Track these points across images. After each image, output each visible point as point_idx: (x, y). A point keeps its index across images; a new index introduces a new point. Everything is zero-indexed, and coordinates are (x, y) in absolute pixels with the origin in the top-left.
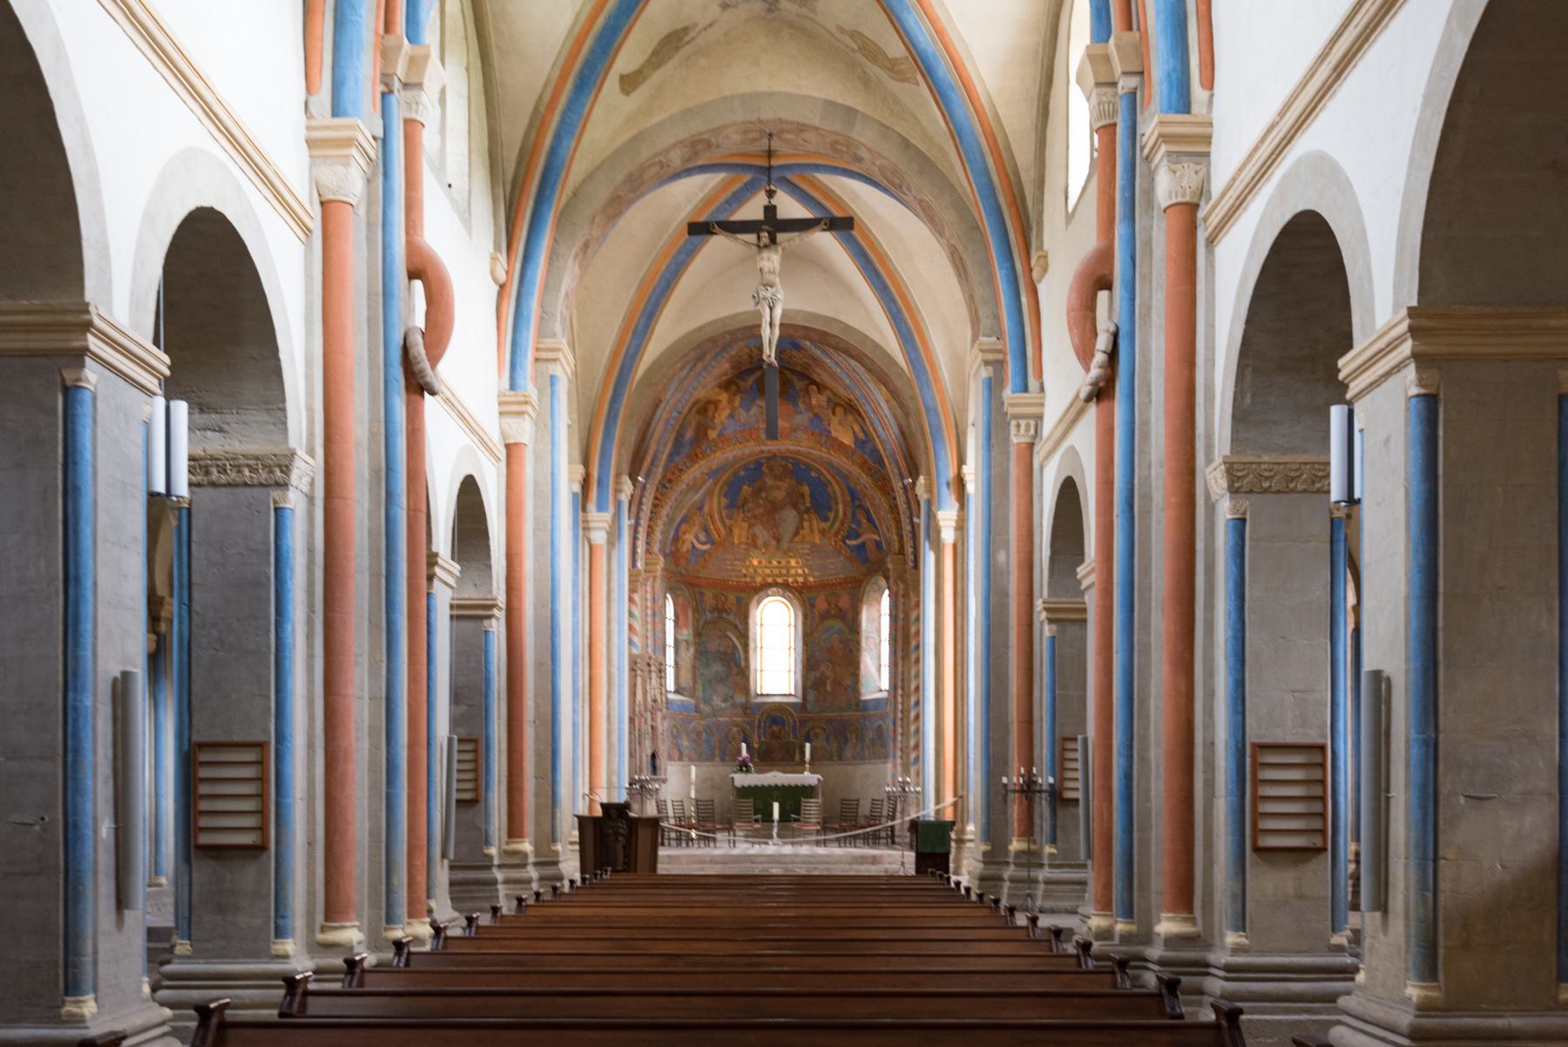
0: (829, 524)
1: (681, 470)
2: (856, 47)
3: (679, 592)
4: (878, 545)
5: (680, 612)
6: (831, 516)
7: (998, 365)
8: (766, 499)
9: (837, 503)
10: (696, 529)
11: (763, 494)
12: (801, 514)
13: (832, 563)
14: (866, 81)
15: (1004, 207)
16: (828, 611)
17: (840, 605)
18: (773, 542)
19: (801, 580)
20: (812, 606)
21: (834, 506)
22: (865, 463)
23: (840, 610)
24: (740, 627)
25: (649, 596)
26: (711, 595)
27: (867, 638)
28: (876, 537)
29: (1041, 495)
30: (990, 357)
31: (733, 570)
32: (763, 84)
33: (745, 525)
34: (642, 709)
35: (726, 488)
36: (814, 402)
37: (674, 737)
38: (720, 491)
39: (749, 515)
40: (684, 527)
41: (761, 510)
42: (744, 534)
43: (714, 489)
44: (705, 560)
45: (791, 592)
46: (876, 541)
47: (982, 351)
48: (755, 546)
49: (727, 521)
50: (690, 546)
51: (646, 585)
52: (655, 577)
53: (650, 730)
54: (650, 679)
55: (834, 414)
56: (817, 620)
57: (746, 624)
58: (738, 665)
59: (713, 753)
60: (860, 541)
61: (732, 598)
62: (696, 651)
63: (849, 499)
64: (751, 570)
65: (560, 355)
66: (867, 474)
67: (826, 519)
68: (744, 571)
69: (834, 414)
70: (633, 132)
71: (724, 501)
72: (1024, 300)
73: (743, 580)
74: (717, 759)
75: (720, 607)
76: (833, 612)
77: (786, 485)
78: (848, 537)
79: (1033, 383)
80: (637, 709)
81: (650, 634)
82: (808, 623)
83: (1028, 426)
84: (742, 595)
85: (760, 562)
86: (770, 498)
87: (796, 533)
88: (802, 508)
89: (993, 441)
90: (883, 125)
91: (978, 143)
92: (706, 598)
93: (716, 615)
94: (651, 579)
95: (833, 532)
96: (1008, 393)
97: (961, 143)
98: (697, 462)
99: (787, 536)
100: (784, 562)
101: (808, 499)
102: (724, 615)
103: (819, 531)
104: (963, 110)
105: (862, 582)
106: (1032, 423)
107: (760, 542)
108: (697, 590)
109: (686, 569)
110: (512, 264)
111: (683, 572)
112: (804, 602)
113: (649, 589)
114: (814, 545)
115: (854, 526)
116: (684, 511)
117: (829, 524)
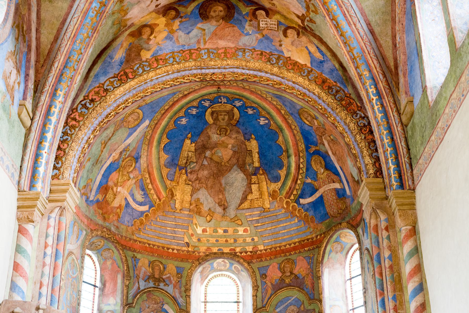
0: (280, 184)
1: (106, 90)
3: (106, 254)
4: (340, 194)
6: (283, 173)
8: (211, 159)
9: (289, 157)
10: (131, 182)
11: (208, 153)
12: (249, 176)
13: (284, 228)
16: (282, 280)
17: (296, 272)
18: (219, 210)
19: (250, 249)
20: (264, 276)
21: (285, 162)
22: (324, 82)
23: (296, 277)
27: (331, 307)
28: (337, 186)
31: (174, 238)
33: (189, 189)
35: (165, 140)
36: (262, 25)
38: (159, 143)
39: (193, 177)
40: (114, 176)
41: (206, 173)
42: (188, 198)
43: (152, 137)
44: (142, 223)
45: (238, 262)
46: (337, 190)
48: (199, 213)
49: (168, 182)
50: (123, 203)
55: (286, 36)
56: (270, 292)
60: (317, 195)
61: (171, 266)
63: (302, 146)
64: (194, 239)
66: (328, 94)
67: (276, 179)
68: (186, 240)
69: (286, 36)
71: (165, 157)
73: (185, 248)
76: (287, 281)
77: (232, 141)
78: (302, 196)
81: (45, 281)
82: (259, 294)
84: (186, 265)
85: (204, 231)
86: (215, 158)
87: (244, 199)
88: (250, 169)
95: (284, 193)
98: (126, 82)
99: (234, 202)
100: (231, 230)
101: (256, 156)
102: (162, 285)
103: (270, 195)
105: (321, 242)
107: (205, 208)
111: (113, 229)
112: (254, 272)
113: (52, 222)
114: (264, 210)
115: (309, 181)
116: (115, 155)
117: (280, 184)
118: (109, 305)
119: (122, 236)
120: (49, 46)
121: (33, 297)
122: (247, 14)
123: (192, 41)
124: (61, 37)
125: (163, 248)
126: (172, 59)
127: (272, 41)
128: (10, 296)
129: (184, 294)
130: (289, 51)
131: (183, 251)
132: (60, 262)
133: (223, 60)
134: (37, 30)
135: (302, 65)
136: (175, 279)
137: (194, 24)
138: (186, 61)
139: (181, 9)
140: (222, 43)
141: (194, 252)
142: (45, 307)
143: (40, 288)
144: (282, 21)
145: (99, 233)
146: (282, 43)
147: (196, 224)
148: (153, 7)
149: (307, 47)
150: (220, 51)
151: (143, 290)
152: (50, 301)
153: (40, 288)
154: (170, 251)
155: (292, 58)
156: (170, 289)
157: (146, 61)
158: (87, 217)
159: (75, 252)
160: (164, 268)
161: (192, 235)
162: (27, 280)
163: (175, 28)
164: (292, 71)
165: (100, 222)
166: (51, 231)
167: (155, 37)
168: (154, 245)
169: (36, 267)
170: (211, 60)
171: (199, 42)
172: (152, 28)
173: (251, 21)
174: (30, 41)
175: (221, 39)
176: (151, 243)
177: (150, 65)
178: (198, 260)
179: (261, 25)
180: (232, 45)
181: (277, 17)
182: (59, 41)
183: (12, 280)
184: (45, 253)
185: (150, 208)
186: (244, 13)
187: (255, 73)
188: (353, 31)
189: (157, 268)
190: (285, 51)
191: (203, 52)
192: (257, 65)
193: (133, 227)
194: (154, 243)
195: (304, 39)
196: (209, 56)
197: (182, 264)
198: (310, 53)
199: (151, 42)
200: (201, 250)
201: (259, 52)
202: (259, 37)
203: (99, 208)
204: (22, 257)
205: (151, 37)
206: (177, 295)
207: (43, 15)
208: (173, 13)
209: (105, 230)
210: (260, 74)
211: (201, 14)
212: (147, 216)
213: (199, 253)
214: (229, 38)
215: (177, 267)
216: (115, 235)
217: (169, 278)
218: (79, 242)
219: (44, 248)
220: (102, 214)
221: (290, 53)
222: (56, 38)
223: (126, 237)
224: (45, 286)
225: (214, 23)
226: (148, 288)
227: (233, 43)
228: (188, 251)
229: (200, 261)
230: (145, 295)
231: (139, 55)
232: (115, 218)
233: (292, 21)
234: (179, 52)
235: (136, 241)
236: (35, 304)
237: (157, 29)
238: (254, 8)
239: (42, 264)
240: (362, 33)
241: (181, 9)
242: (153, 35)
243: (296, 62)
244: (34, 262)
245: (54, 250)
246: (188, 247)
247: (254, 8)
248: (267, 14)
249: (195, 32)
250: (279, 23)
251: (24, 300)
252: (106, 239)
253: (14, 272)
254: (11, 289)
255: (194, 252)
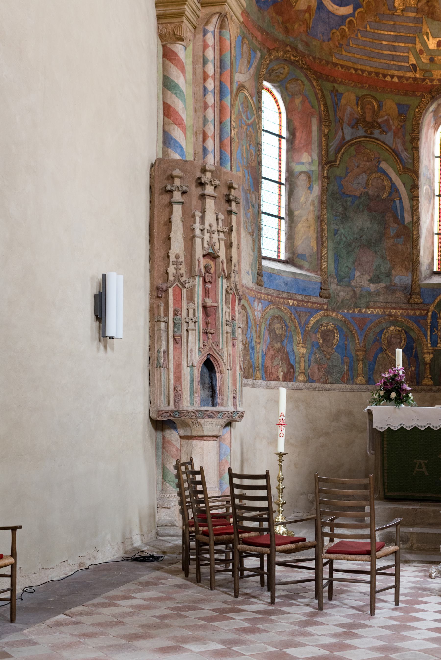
5: (297, 123)
24: (405, 155)
25: (210, 54)
26: (353, 98)
34: (183, 270)
37: (275, 337)
44: (343, 35)
51: (205, 33)
52: (223, 17)
53: (200, 313)
54: (203, 212)
57: (417, 149)
58: (399, 221)
59: (351, 368)
62: (324, 190)
64: (425, 59)
68: (412, 61)
74: (360, 379)
75: (369, 119)
80: (172, 270)
81: (211, 129)
92: (343, 101)
93: (361, 132)
94: (215, 19)
108: (328, 85)
109: (307, 44)
111: (300, 47)
118: (303, 163)
119: (314, 58)
121: (195, 155)
125: (377, 74)
128: (165, 153)
129: (409, 146)
131: (408, 79)
132: (227, 101)
136: (396, 123)
141: (424, 80)
142: (213, 168)
143: (204, 141)
145: (281, 54)
147: (427, 34)
151: (349, 141)
152: (219, 159)
153: (204, 141)
154: (388, 79)
156: (389, 138)
158: (260, 28)
159: (247, 85)
160: (380, 107)
161: (421, 52)
162: (184, 130)
165: (281, 36)
166: (210, 54)
168: (363, 71)
169: (195, 110)
176: (359, 67)
178: (430, 92)
183: (164, 131)
184: (205, 89)
185: (355, 9)
189: (369, 106)
193: (331, 43)
194: (363, 68)
197: (406, 100)
200: (435, 76)
203: (277, 13)
204: (174, 96)
206: (400, 147)
209: (288, 48)
212: (351, 22)
213: (432, 80)
215: (398, 105)
216: (303, 56)
217: (387, 121)
218: (252, 70)
219: (202, 82)
220: (283, 23)
223: (321, 60)
224: (210, 138)
226: (356, 138)
228: (415, 79)
229: (434, 94)
230: (353, 148)
232: (303, 29)
235: (336, 65)
236: (199, 163)
239: (202, 104)
244: (190, 101)
245: (217, 83)
246: (416, 71)
251: (184, 159)
252: (292, 63)
253: (166, 119)
254: (164, 143)
255: (424, 80)
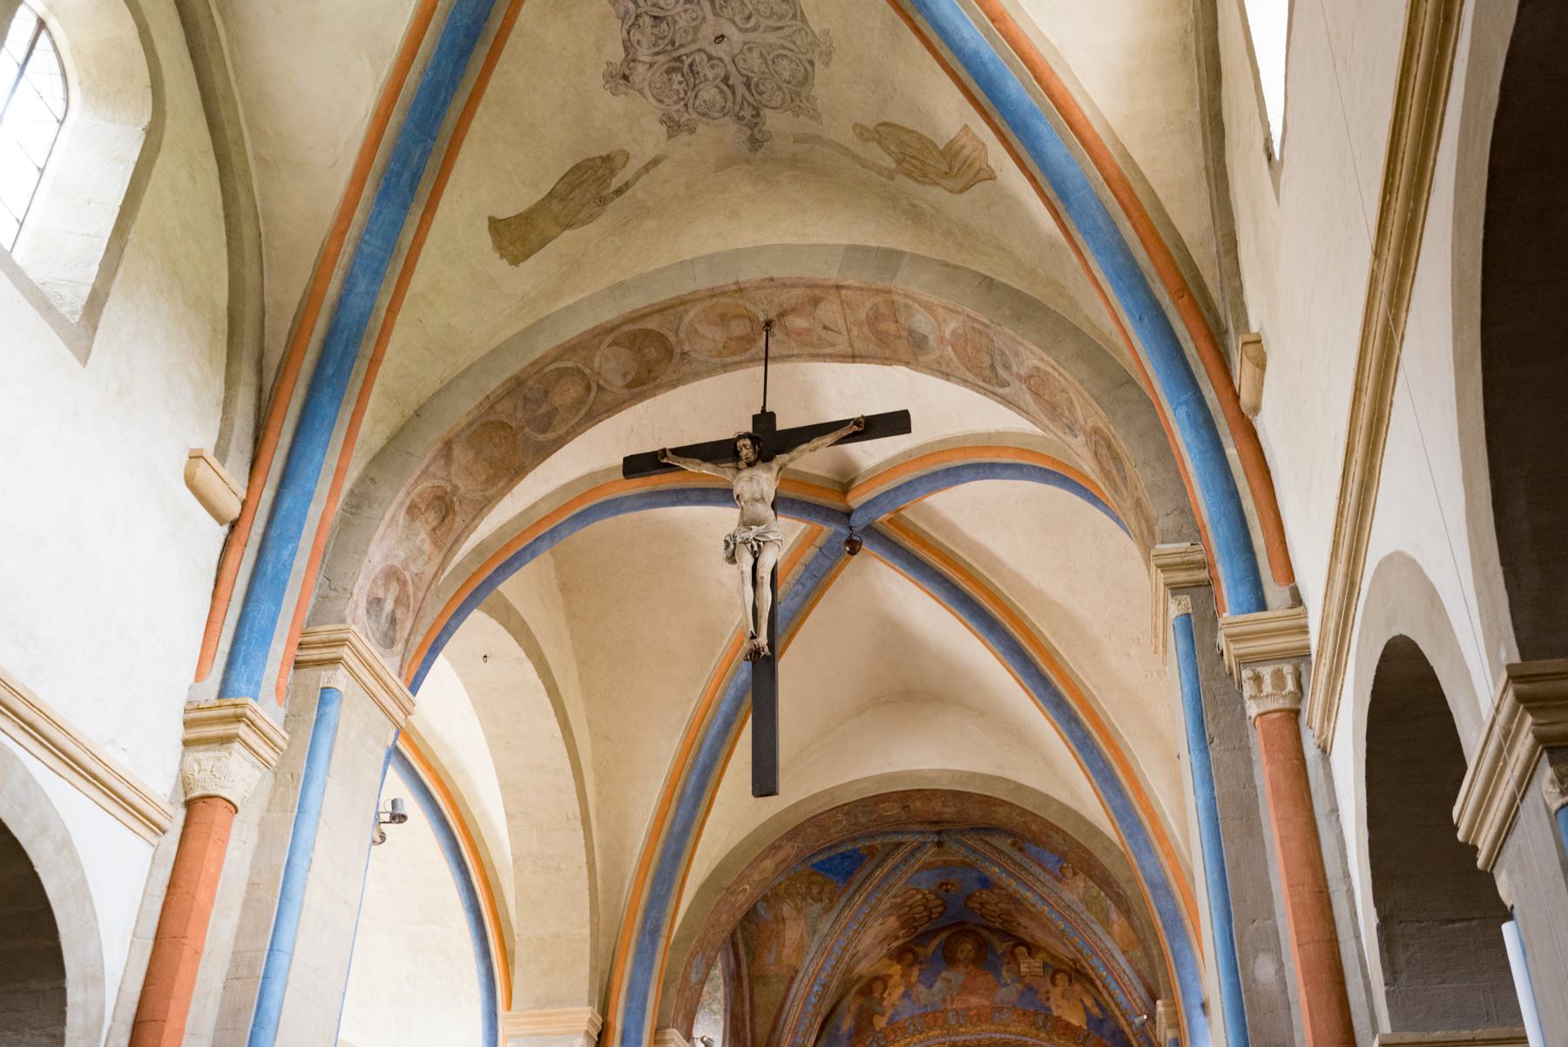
2: (889, 163)
7: (1202, 590)
14: (916, 216)
15: (1166, 302)
29: (1335, 810)
30: (1181, 577)
32: (745, 237)
47: (1164, 568)
65: (345, 652)
70: (530, 321)
72: (1231, 452)
79: (1275, 593)
83: (1279, 678)
89: (1210, 729)
90: (947, 265)
91: (1102, 205)
96: (1230, 617)
97: (1069, 208)
104: (1060, 148)
106: (1287, 669)
110: (256, 491)
120: (766, 1039)
122: (1003, 953)
123: (936, 999)
124: (779, 1029)
126: (912, 1028)
127: (1036, 993)
130: (1058, 1007)
133: (976, 1025)
134: (752, 1021)
135: (1076, 1027)
137: (939, 972)
138: (931, 1029)
139: (919, 950)
140: (974, 1001)
144: (1049, 961)
146: (1050, 995)
148: (884, 951)
149: (1081, 1001)
150: (972, 1013)
155: (1063, 1018)
157: (881, 1032)
163: (914, 979)
164: (1063, 1037)
167: (890, 995)
170: (961, 1026)
171: (944, 1000)
172: (884, 980)
173: (1008, 963)
174: (745, 1038)
175: (971, 993)
177: (885, 1038)
179: (1022, 970)
180: (988, 1003)
181: (1042, 955)
182: (777, 1033)
186: (1000, 952)
187: (1018, 1038)
188: (1129, 1001)
190: (1053, 1008)
191: (950, 1014)
192: (1019, 1029)
195: (1077, 987)
196: (958, 1021)
198: (1085, 1008)
199: (885, 1004)
201: (1021, 1012)
202: (1020, 987)
205: (885, 995)
207: (757, 1000)
208: (910, 956)
210: (1024, 1039)
211: (945, 957)
214: (982, 991)
221: (1060, 1010)
222: (774, 1029)
225: (963, 970)
227: (987, 999)
231: (871, 1023)
233: (1060, 960)
234: (920, 1016)
237: (891, 983)
238: (1012, 943)
240: (1140, 1005)
241: (919, 950)
242: (887, 992)
243: (1069, 1024)
247: (1012, 943)
248: (1030, 953)
249: (939, 985)
250: (1045, 965)
